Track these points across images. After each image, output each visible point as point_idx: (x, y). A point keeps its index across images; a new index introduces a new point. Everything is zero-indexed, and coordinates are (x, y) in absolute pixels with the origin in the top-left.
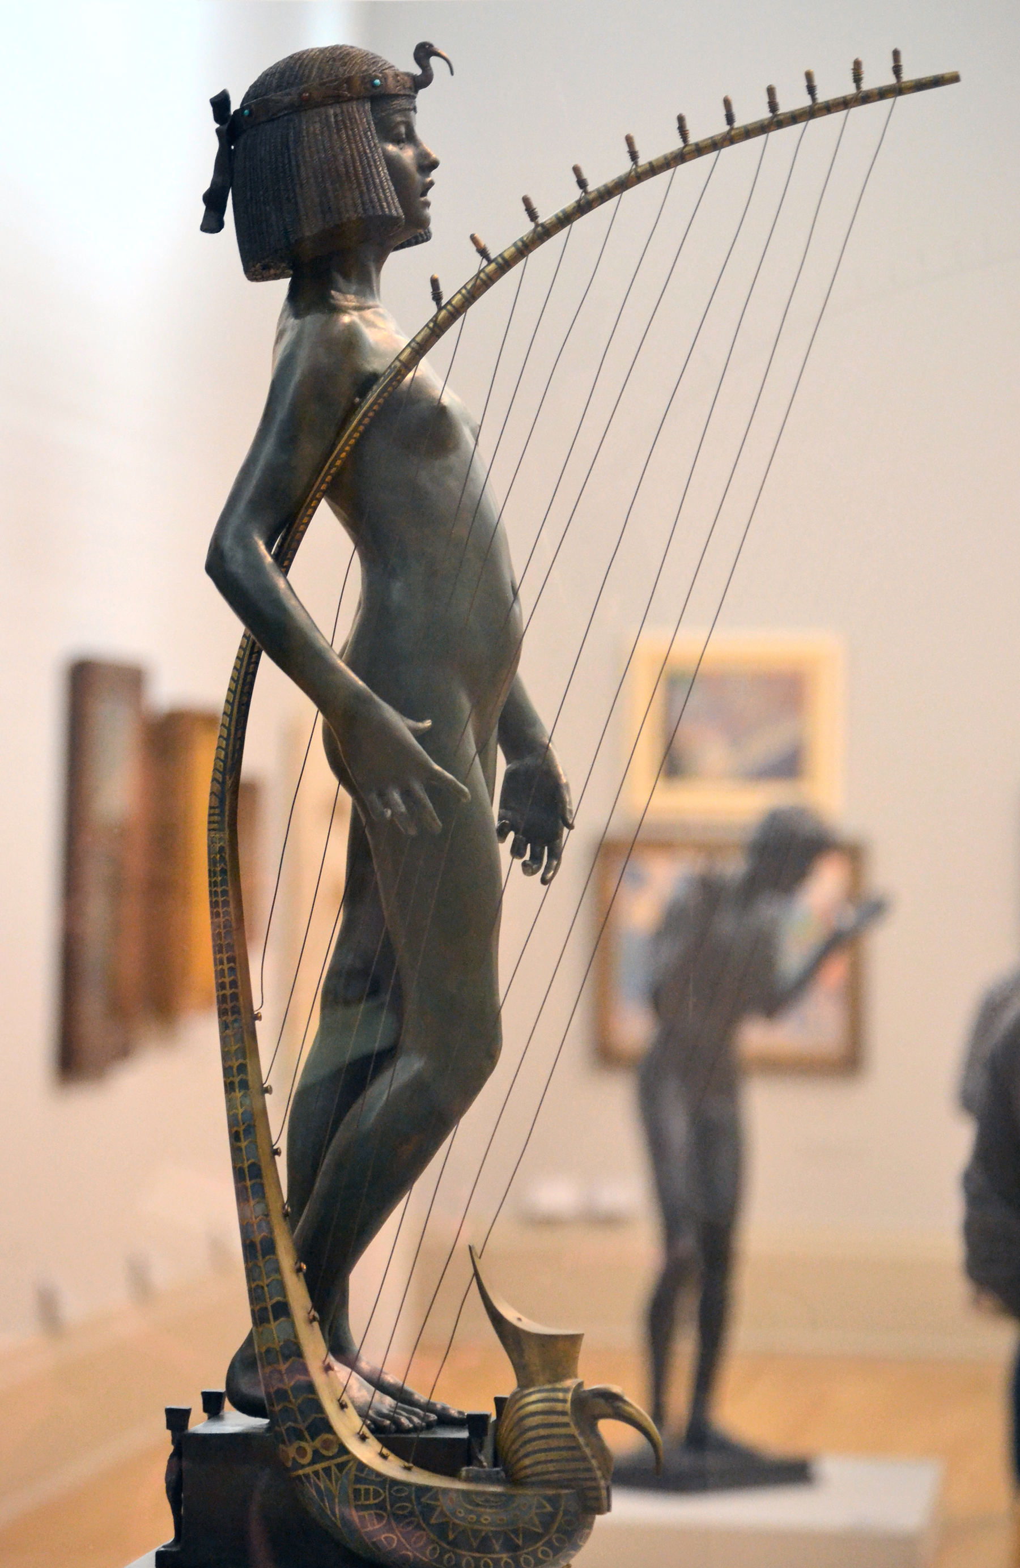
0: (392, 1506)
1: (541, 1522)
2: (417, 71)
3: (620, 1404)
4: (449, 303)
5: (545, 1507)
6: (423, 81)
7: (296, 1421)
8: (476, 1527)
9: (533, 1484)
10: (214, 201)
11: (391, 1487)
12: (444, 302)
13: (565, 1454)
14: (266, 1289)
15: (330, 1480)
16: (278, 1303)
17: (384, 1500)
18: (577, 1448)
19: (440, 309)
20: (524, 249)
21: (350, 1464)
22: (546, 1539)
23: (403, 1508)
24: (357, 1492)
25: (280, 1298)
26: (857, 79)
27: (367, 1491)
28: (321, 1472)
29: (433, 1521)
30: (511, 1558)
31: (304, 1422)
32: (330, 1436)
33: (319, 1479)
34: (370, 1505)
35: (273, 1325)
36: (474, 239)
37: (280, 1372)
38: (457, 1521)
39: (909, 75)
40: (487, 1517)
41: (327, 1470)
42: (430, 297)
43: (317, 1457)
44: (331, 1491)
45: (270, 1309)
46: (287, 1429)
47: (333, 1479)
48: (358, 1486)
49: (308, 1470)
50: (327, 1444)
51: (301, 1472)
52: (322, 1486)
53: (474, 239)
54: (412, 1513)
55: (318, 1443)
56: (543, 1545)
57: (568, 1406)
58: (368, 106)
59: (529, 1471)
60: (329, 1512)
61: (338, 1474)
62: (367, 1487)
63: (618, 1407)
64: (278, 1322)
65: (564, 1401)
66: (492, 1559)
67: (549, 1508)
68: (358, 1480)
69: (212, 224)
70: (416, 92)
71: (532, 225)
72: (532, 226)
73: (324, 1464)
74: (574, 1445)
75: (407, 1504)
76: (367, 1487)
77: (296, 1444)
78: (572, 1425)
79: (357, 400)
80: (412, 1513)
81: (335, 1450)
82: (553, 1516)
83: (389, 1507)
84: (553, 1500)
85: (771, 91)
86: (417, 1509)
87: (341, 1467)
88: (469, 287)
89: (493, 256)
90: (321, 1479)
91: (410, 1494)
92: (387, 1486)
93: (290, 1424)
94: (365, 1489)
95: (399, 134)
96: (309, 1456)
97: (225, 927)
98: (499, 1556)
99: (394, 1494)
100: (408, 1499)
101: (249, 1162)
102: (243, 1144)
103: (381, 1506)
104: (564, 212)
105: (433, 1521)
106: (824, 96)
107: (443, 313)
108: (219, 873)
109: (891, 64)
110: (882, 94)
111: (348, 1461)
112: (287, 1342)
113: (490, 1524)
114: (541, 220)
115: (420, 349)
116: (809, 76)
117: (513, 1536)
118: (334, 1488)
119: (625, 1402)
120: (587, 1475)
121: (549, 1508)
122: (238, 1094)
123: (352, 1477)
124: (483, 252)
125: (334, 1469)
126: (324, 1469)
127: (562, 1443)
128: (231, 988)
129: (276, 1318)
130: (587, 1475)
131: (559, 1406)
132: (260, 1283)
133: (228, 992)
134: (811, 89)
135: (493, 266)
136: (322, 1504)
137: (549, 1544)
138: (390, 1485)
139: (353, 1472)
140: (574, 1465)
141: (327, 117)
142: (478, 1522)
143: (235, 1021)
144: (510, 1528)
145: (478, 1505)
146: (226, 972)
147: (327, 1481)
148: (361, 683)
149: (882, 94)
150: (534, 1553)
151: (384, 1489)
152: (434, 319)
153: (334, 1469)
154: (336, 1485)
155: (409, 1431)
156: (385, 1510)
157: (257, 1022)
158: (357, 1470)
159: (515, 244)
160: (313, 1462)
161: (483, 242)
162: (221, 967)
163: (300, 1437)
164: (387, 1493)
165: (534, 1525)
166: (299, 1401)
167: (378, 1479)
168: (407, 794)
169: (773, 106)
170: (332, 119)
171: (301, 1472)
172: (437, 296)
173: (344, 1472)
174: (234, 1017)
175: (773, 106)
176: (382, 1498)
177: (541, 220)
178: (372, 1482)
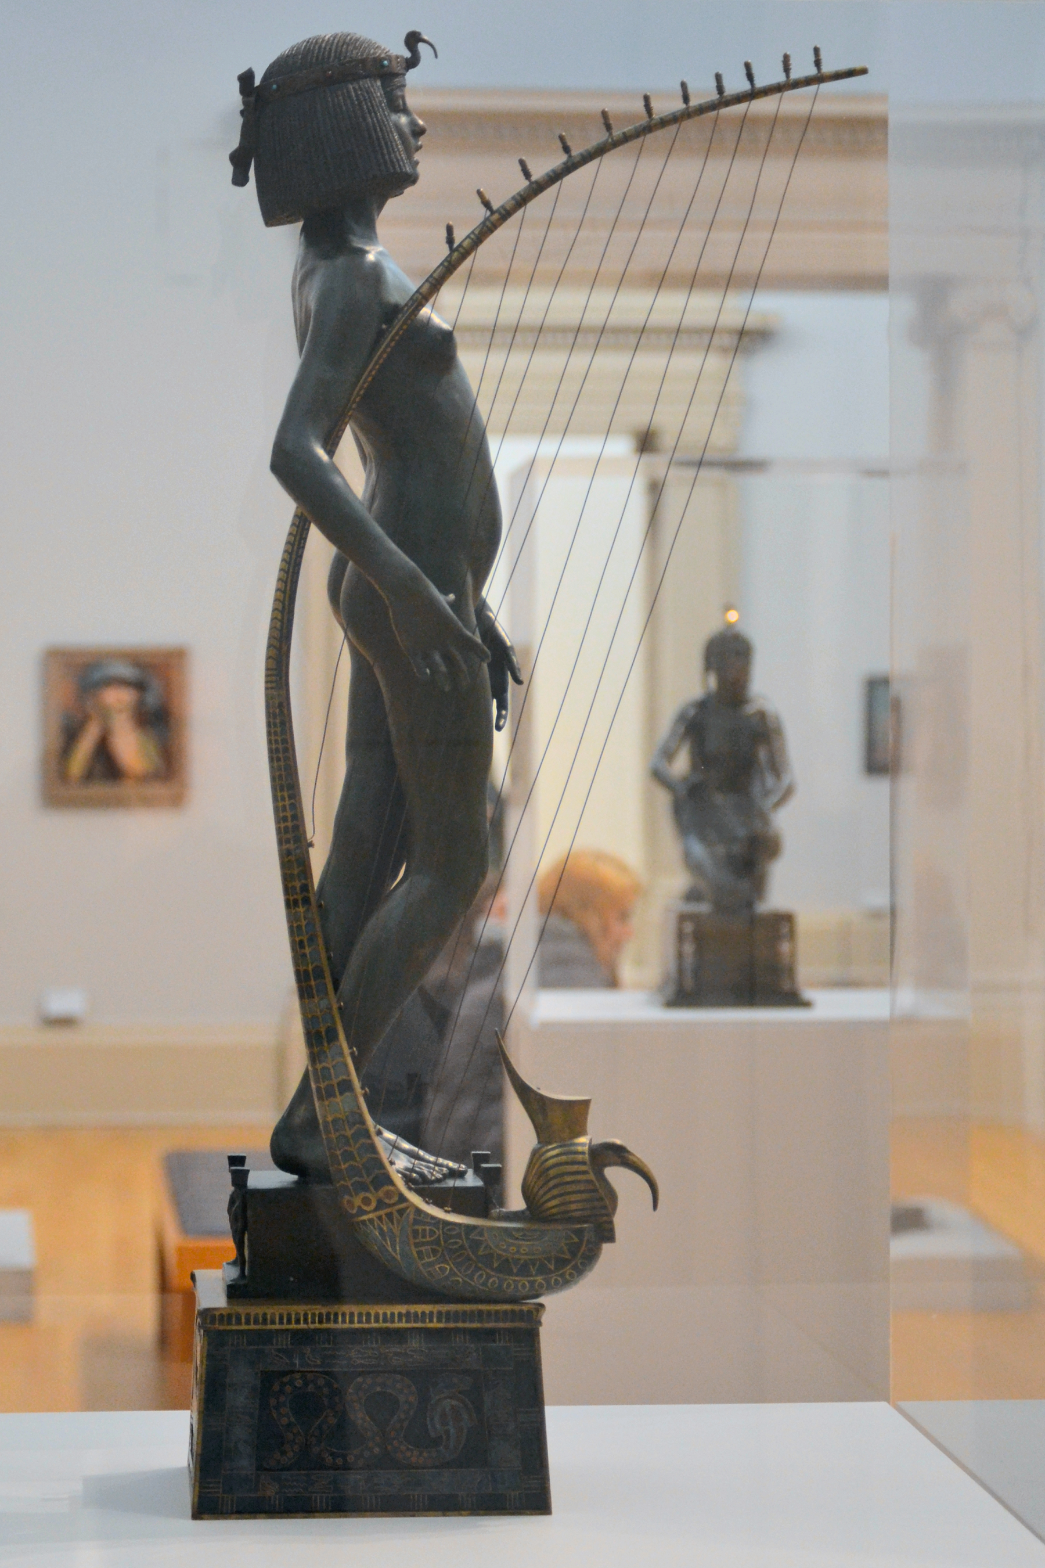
0: (445, 1242)
2: (407, 54)
4: (460, 245)
5: (573, 1239)
6: (412, 62)
7: (361, 1176)
8: (517, 1256)
9: (556, 1221)
10: (239, 161)
11: (443, 1228)
12: (455, 245)
13: (584, 1196)
14: (332, 1071)
15: (393, 1223)
16: (344, 1080)
17: (439, 1237)
18: (595, 1191)
19: (452, 250)
20: (521, 201)
21: (408, 1211)
22: (573, 1263)
23: (456, 1243)
24: (415, 1233)
25: (344, 1077)
26: (787, 69)
27: (424, 1230)
28: (384, 1217)
29: (480, 1253)
32: (391, 1188)
33: (382, 1222)
35: (339, 1099)
36: (480, 193)
38: (500, 1252)
39: (827, 68)
40: (525, 1248)
41: (389, 1216)
42: (444, 240)
43: (381, 1204)
44: (393, 1233)
45: (336, 1085)
46: (352, 1185)
47: (395, 1222)
48: (416, 1227)
49: (371, 1216)
50: (388, 1194)
51: (365, 1217)
52: (385, 1228)
53: (480, 193)
54: (462, 1247)
55: (381, 1194)
57: (587, 1156)
58: (379, 83)
59: (554, 1211)
60: (390, 1249)
61: (399, 1218)
64: (343, 1097)
65: (583, 1153)
67: (576, 1240)
68: (416, 1222)
69: (240, 180)
70: (407, 71)
71: (527, 183)
72: (527, 183)
73: (388, 1210)
74: (593, 1188)
75: (458, 1240)
76: (423, 1227)
77: (362, 1195)
78: (591, 1173)
79: (384, 326)
80: (462, 1247)
81: (396, 1198)
82: (578, 1246)
83: (442, 1243)
85: (718, 78)
86: (467, 1245)
87: (401, 1212)
88: (477, 232)
89: (495, 206)
90: (384, 1222)
92: (441, 1226)
93: (357, 1178)
95: (399, 106)
96: (374, 1204)
97: (286, 770)
99: (448, 1233)
100: (459, 1236)
101: (314, 965)
102: (307, 951)
103: (437, 1242)
104: (553, 171)
105: (480, 1253)
106: (760, 83)
107: (456, 254)
108: (278, 725)
109: (812, 58)
110: (808, 81)
111: (407, 1208)
112: (353, 1113)
113: (526, 1254)
114: (534, 178)
115: (435, 284)
116: (748, 66)
117: (546, 1262)
118: (396, 1231)
119: (628, 1152)
120: (603, 1212)
121: (576, 1240)
122: (301, 909)
124: (487, 204)
125: (396, 1215)
126: (387, 1215)
127: (582, 1187)
128: (292, 821)
129: (341, 1094)
130: (603, 1212)
131: (580, 1157)
132: (327, 1065)
133: (290, 824)
134: (750, 77)
135: (496, 216)
136: (384, 1243)
137: (575, 1267)
138: (443, 1224)
139: (412, 1216)
141: (348, 92)
142: (518, 1252)
143: (297, 848)
145: (517, 1239)
146: (288, 807)
147: (390, 1224)
148: (412, 564)
149: (808, 81)
150: (562, 1275)
151: (438, 1229)
152: (448, 259)
153: (396, 1215)
154: (398, 1228)
155: (433, 1182)
156: (439, 1244)
157: (311, 850)
159: (513, 198)
160: (376, 1209)
161: (488, 196)
162: (283, 803)
165: (563, 1253)
166: (364, 1160)
167: (433, 1222)
168: (448, 658)
169: (720, 89)
170: (353, 94)
171: (365, 1217)
172: (450, 240)
173: (405, 1215)
174: (296, 845)
175: (720, 89)
176: (436, 1236)
177: (534, 178)
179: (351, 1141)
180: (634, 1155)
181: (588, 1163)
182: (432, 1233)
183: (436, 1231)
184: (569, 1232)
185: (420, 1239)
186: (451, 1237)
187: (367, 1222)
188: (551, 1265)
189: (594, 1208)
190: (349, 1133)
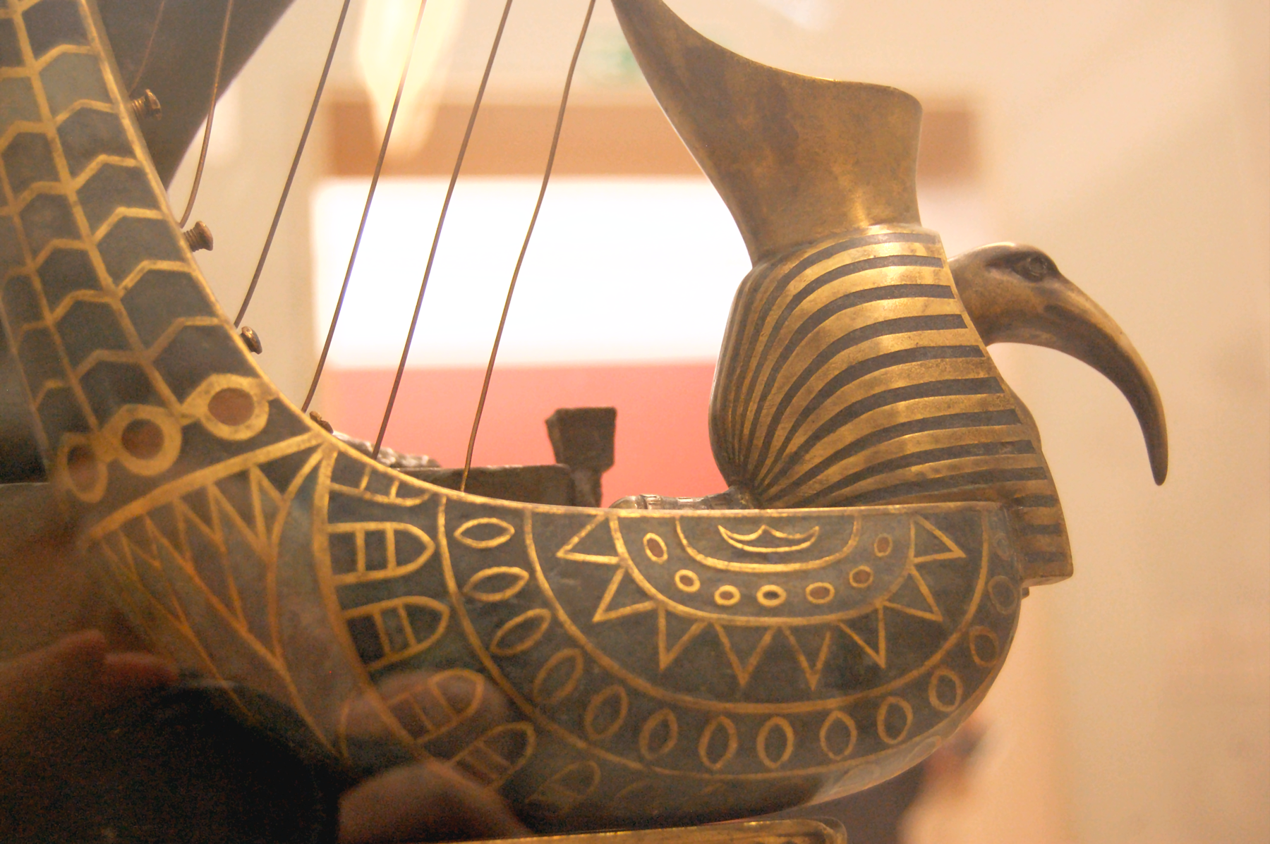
1: (937, 595)
3: (1056, 285)
8: (741, 620)
24: (342, 546)
27: (375, 539)
28: (213, 492)
30: (852, 710)
31: (147, 344)
34: (386, 582)
37: (60, 203)
55: (197, 405)
56: (943, 663)
60: (242, 629)
61: (274, 493)
62: (372, 526)
63: (1051, 293)
66: (792, 719)
68: (343, 507)
74: (982, 375)
75: (515, 570)
76: (372, 526)
77: (122, 417)
81: (259, 420)
83: (451, 584)
84: (962, 527)
87: (280, 472)
91: (518, 539)
92: (441, 520)
93: (100, 355)
94: (369, 535)
98: (819, 705)
111: (309, 452)
121: (957, 553)
123: (322, 500)
136: (215, 601)
139: (324, 481)
140: (986, 433)
142: (749, 602)
144: (852, 614)
154: (269, 529)
156: (440, 592)
158: (335, 478)
163: (139, 390)
164: (444, 541)
165: (919, 601)
167: (409, 502)
178: (392, 512)
179: (79, 215)
180: (1080, 292)
181: (954, 290)
182: (409, 545)
183: (425, 538)
184: (928, 525)
185: (360, 573)
186: (490, 557)
187: (149, 523)
188: (877, 650)
189: (988, 448)
190: (70, 185)
